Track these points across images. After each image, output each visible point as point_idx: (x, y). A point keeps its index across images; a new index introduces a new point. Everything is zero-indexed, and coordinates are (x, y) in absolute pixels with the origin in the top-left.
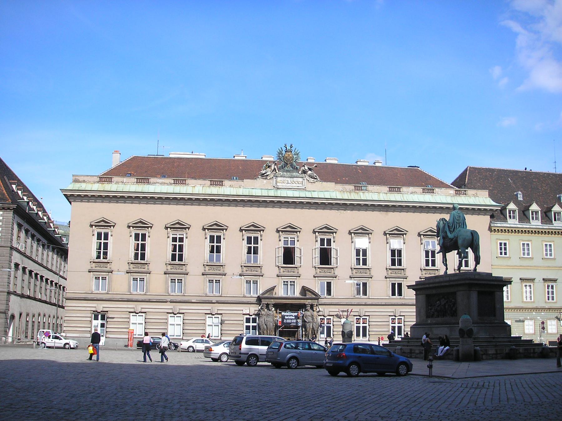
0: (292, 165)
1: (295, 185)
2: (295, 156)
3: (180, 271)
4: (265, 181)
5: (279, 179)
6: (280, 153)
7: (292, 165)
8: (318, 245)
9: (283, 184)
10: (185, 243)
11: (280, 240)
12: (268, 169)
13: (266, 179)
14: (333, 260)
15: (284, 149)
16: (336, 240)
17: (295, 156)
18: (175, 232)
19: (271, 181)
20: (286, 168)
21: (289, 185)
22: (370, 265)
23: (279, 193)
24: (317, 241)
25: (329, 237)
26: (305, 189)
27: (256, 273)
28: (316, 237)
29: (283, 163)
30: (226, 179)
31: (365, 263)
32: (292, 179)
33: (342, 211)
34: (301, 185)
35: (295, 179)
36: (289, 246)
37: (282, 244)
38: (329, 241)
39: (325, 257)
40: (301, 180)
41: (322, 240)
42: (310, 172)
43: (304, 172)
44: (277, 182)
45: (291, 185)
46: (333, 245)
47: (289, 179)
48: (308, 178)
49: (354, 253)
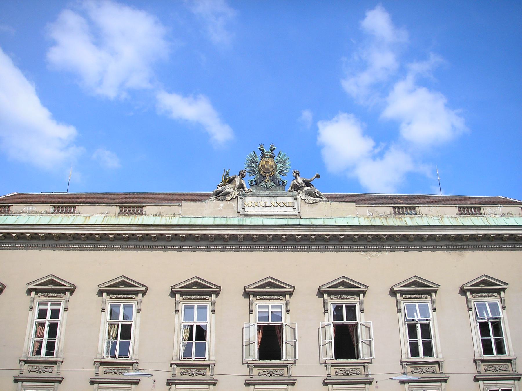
1: (278, 209)
2: (279, 165)
3: (47, 375)
4: (222, 204)
5: (248, 199)
6: (252, 161)
8: (329, 319)
9: (257, 209)
10: (62, 320)
11: (251, 312)
12: (230, 186)
13: (224, 200)
14: (363, 349)
16: (365, 307)
17: (279, 165)
18: (44, 300)
19: (233, 203)
20: (263, 184)
21: (267, 209)
22: (440, 356)
23: (248, 221)
24: (326, 311)
25: (350, 302)
26: (298, 215)
27: (200, 377)
28: (325, 303)
29: (258, 175)
30: (149, 203)
31: (428, 350)
32: (273, 199)
33: (374, 253)
34: (290, 209)
35: (279, 199)
36: (270, 321)
37: (254, 320)
38: (351, 310)
39: (346, 343)
40: (290, 199)
41: (338, 310)
42: (306, 188)
43: (297, 188)
45: (272, 209)
46: (360, 318)
47: (267, 200)
48: (302, 195)
49: (405, 332)
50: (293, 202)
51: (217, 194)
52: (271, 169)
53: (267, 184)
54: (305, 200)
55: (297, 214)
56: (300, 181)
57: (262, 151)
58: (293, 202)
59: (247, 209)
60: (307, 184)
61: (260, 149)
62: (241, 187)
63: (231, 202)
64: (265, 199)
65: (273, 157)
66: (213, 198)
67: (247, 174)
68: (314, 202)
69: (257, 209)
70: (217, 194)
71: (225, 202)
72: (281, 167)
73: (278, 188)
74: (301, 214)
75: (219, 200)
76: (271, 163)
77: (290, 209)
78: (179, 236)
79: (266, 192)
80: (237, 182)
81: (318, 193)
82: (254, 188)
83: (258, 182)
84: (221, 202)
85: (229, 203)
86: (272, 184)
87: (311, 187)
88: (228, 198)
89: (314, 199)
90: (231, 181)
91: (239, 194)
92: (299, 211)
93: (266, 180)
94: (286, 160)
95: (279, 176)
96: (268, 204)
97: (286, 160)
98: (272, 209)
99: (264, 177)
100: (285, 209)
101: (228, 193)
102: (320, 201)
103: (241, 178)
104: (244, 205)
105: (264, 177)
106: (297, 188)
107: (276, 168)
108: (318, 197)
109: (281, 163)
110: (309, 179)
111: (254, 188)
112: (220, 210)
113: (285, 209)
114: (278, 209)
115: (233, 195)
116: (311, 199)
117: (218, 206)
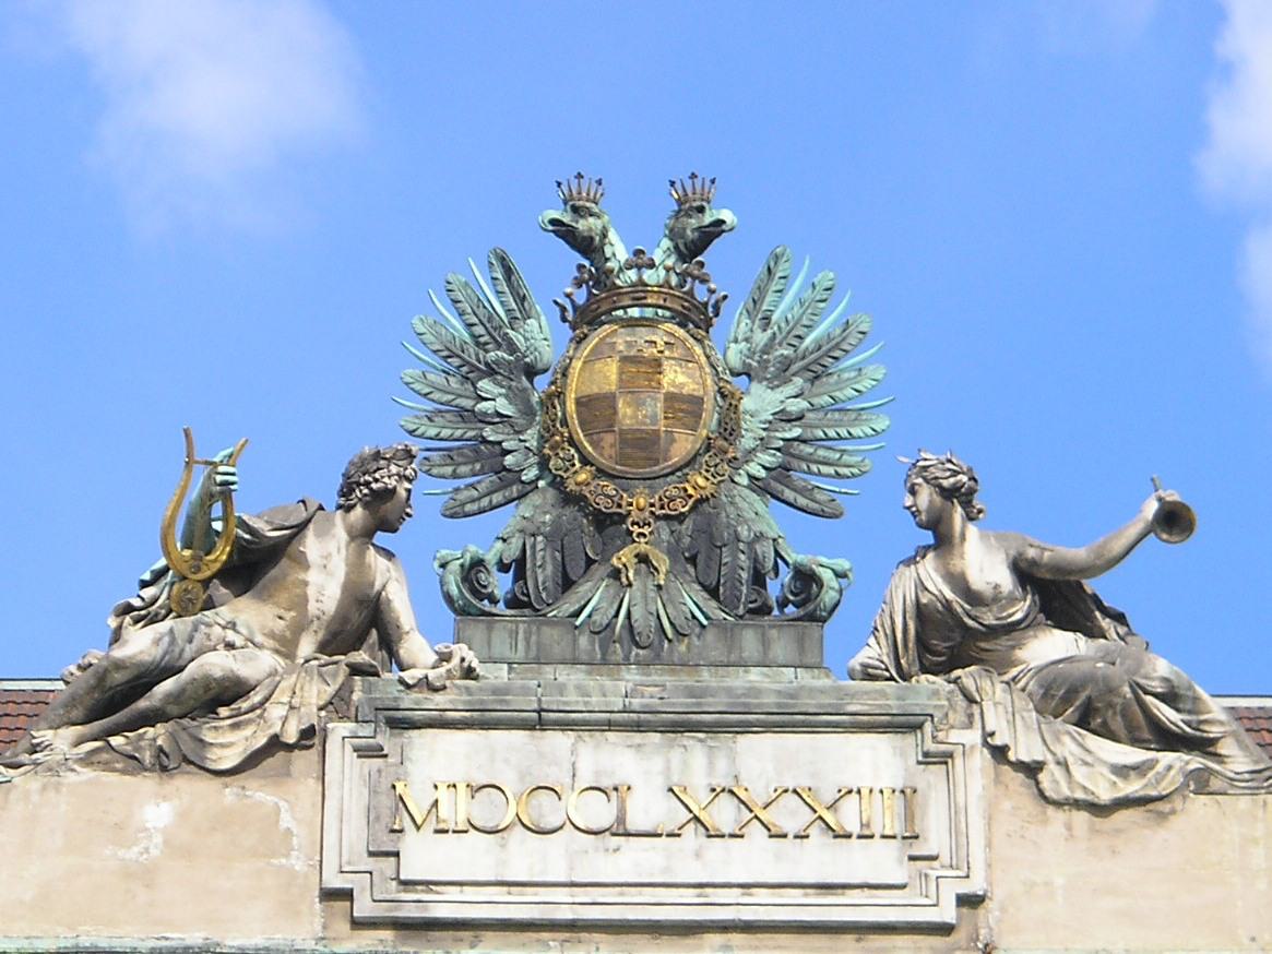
0: (703, 548)
1: (753, 858)
2: (760, 402)
4: (158, 806)
5: (438, 761)
6: (487, 355)
7: (703, 548)
9: (524, 857)
12: (248, 614)
15: (554, 274)
17: (760, 402)
19: (279, 800)
20: (595, 596)
21: (634, 859)
29: (539, 508)
32: (696, 762)
34: (881, 861)
35: (762, 760)
40: (875, 761)
42: (1051, 646)
43: (948, 640)
44: (390, 822)
45: (689, 859)
47: (643, 770)
48: (1005, 712)
50: (908, 794)
51: (114, 701)
52: (683, 445)
53: (640, 602)
54: (1032, 770)
55: (947, 913)
56: (985, 564)
57: (588, 247)
58: (908, 794)
59: (422, 856)
60: (1060, 596)
61: (562, 230)
62: (363, 625)
63: (258, 792)
64: (616, 757)
65: (697, 317)
66: (61, 740)
67: (427, 494)
68: (1133, 787)
69: (524, 857)
70: (114, 701)
71: (190, 788)
72: (786, 418)
73: (749, 640)
74: (990, 914)
75: (133, 764)
76: (675, 377)
77: (881, 861)
78: (589, 323)
79: (623, 687)
80: (325, 570)
81: (1171, 697)
82: (501, 643)
83: (543, 573)
84: (147, 783)
85: (228, 794)
86: (691, 599)
87: (1093, 632)
88: (229, 742)
89: (1135, 755)
90: (253, 564)
91: (338, 705)
92: (974, 886)
93: (625, 557)
94: (832, 350)
95: (763, 519)
96: (648, 808)
97: (832, 350)
98: (689, 859)
99: (608, 524)
100: (819, 860)
101: (224, 695)
102: (1200, 783)
103: (363, 536)
104: (390, 822)
105: (608, 524)
106: (948, 640)
107: (729, 428)
108: (1169, 740)
109: (783, 373)
110: (1078, 553)
111: (501, 645)
112: (145, 875)
113: (819, 860)
114: (753, 858)
115: (275, 712)
116: (1097, 764)
117: (120, 831)
